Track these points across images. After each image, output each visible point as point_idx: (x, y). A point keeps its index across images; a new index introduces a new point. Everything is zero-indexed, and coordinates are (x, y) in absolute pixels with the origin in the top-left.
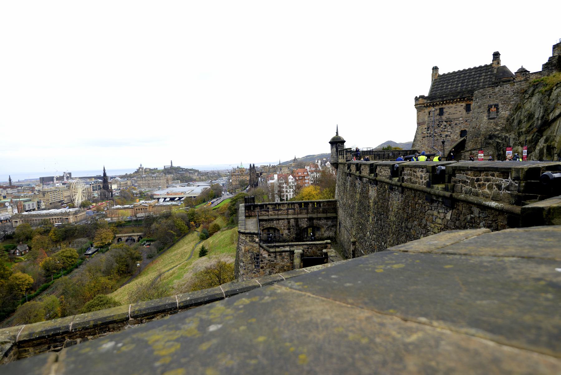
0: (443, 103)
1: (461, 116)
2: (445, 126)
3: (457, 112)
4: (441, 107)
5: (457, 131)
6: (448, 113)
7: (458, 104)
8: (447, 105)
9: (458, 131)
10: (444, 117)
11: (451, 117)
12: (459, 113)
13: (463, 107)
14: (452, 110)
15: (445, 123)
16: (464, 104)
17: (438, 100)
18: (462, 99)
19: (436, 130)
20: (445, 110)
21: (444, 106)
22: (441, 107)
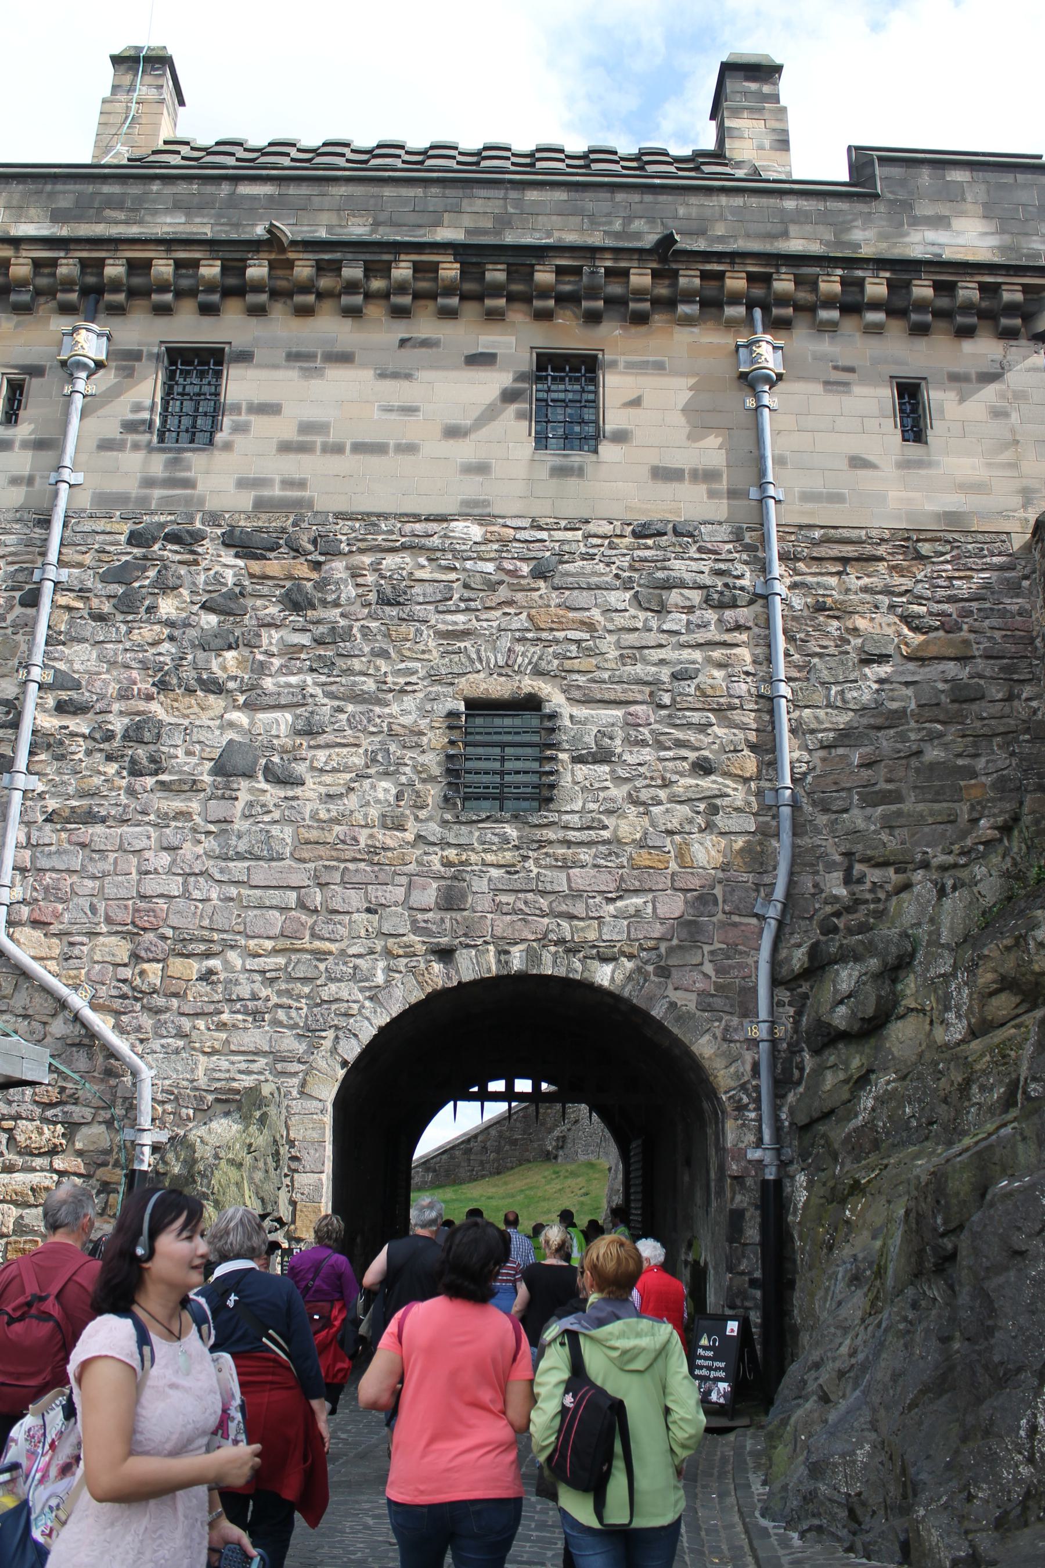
0: (234, 287)
1: (472, 488)
2: (226, 604)
3: (411, 429)
4: (187, 328)
5: (404, 711)
6: (284, 428)
7: (425, 325)
8: (282, 327)
9: (421, 715)
10: (223, 479)
11: (334, 485)
12: (435, 447)
13: (493, 383)
14: (344, 396)
15: (229, 567)
16: (516, 341)
17: (169, 224)
18: (490, 278)
19: (80, 659)
20: (239, 385)
21: (231, 328)
22: (187, 328)
